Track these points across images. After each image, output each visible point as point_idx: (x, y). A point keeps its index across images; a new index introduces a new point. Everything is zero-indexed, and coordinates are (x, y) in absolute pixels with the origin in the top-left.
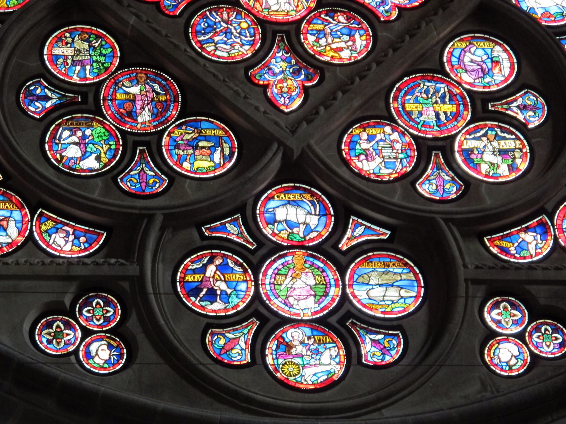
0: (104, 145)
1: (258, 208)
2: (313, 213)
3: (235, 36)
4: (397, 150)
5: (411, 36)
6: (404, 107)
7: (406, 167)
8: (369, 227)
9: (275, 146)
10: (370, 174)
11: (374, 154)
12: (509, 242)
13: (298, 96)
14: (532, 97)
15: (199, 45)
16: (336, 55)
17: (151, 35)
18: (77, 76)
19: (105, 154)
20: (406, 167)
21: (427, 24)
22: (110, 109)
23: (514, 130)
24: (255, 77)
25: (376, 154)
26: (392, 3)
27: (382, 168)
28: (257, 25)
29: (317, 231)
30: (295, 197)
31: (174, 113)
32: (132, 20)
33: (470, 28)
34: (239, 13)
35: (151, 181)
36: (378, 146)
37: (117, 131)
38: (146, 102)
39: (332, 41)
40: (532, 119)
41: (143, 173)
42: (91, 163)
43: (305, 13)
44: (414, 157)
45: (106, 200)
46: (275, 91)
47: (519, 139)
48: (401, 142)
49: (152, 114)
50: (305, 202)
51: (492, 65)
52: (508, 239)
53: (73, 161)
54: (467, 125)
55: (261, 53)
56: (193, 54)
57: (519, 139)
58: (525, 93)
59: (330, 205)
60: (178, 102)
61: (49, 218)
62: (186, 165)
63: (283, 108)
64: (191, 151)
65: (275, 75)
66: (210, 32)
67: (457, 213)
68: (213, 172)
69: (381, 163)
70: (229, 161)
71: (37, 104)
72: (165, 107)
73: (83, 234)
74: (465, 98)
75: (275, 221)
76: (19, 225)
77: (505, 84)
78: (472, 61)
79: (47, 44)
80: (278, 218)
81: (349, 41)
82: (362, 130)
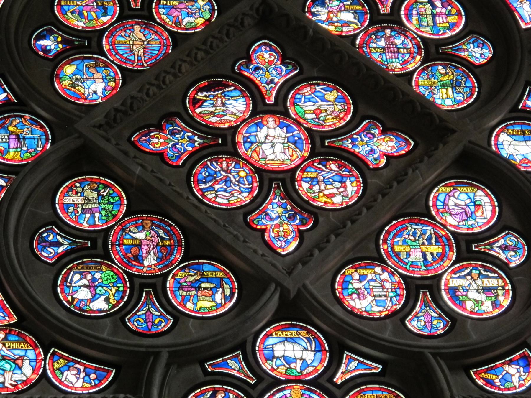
0: (112, 288)
1: (258, 345)
2: (309, 349)
3: (234, 184)
4: (388, 289)
5: (399, 182)
6: (393, 249)
7: (396, 305)
8: (362, 362)
9: (273, 287)
10: (362, 312)
11: (366, 293)
12: (493, 375)
13: (294, 239)
14: (513, 238)
15: (200, 192)
16: (329, 200)
17: (155, 184)
18: (87, 223)
19: (114, 296)
20: (396, 305)
21: (413, 171)
22: (118, 254)
23: (497, 269)
24: (253, 222)
25: (368, 293)
26: (380, 151)
27: (373, 306)
28: (254, 174)
29: (313, 366)
30: (292, 335)
31: (178, 256)
32: (138, 170)
33: (454, 174)
34: (237, 163)
35: (157, 321)
36: (369, 286)
37: (124, 274)
38: (152, 246)
39: (325, 188)
40: (513, 259)
41: (149, 313)
42: (100, 304)
43: (299, 162)
44: (403, 295)
45: (114, 339)
46: (273, 235)
47: (501, 277)
48: (390, 281)
49: (158, 258)
50: (302, 339)
51: (475, 209)
52: (493, 371)
53: (84, 303)
54: (453, 264)
55: (259, 200)
56: (195, 201)
57: (501, 277)
58: (506, 234)
59: (325, 342)
60: (181, 246)
61: (62, 357)
62: (189, 305)
63: (279, 250)
64: (193, 293)
65: (272, 219)
66: (211, 181)
67: (444, 348)
68: (215, 312)
69: (372, 301)
70: (230, 301)
71: (49, 249)
72: (169, 251)
73: (93, 371)
74: (450, 240)
75: (273, 357)
76: (33, 364)
77: (488, 226)
78: (456, 205)
79: (59, 194)
80: (277, 354)
81: (340, 187)
82: (354, 270)
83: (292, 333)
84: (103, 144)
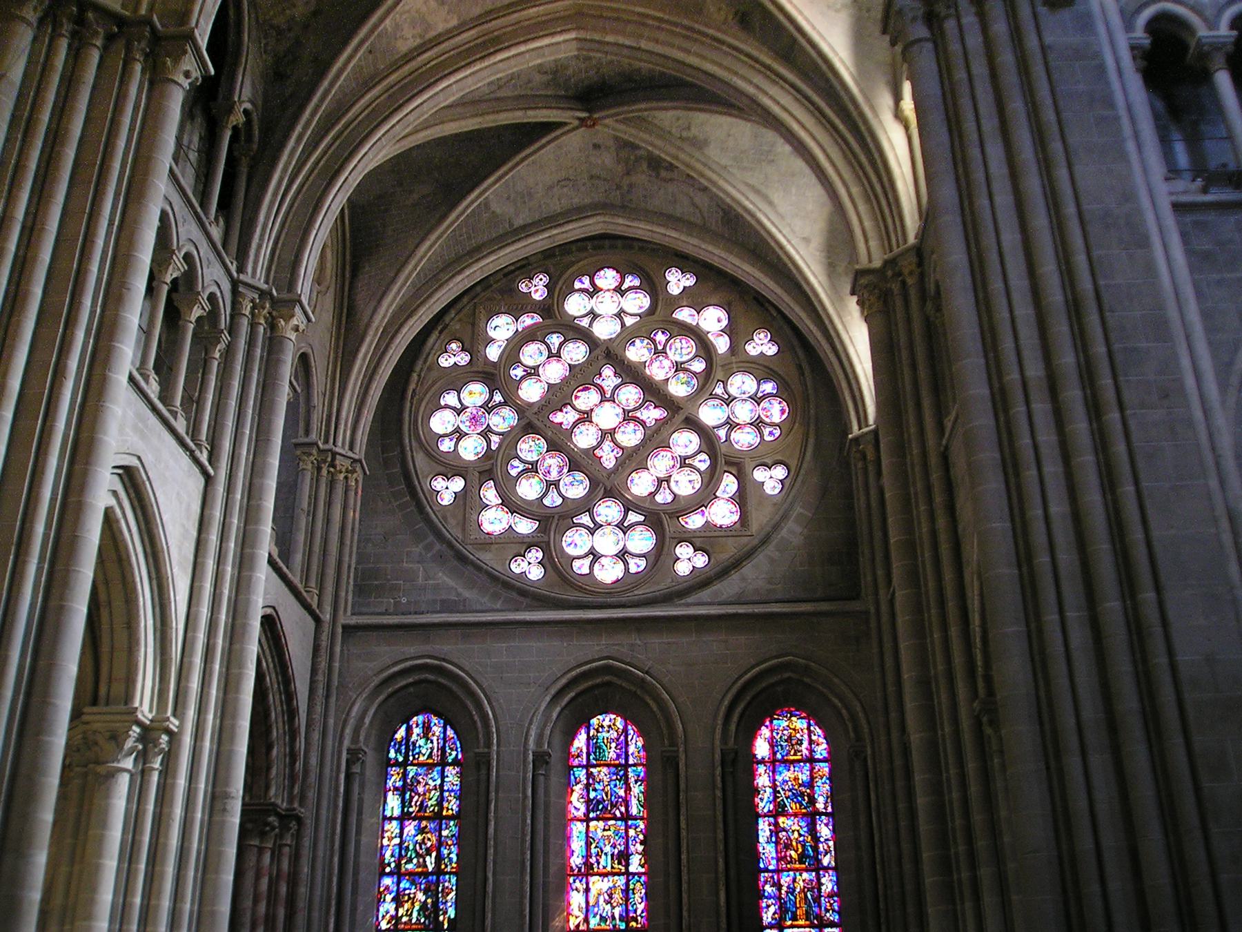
83: (609, 503)
84: (536, 422)
